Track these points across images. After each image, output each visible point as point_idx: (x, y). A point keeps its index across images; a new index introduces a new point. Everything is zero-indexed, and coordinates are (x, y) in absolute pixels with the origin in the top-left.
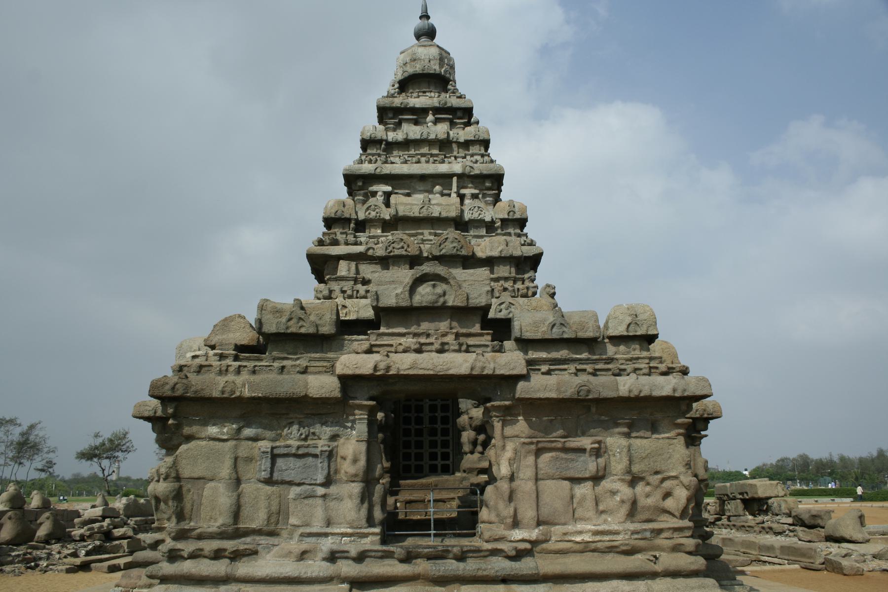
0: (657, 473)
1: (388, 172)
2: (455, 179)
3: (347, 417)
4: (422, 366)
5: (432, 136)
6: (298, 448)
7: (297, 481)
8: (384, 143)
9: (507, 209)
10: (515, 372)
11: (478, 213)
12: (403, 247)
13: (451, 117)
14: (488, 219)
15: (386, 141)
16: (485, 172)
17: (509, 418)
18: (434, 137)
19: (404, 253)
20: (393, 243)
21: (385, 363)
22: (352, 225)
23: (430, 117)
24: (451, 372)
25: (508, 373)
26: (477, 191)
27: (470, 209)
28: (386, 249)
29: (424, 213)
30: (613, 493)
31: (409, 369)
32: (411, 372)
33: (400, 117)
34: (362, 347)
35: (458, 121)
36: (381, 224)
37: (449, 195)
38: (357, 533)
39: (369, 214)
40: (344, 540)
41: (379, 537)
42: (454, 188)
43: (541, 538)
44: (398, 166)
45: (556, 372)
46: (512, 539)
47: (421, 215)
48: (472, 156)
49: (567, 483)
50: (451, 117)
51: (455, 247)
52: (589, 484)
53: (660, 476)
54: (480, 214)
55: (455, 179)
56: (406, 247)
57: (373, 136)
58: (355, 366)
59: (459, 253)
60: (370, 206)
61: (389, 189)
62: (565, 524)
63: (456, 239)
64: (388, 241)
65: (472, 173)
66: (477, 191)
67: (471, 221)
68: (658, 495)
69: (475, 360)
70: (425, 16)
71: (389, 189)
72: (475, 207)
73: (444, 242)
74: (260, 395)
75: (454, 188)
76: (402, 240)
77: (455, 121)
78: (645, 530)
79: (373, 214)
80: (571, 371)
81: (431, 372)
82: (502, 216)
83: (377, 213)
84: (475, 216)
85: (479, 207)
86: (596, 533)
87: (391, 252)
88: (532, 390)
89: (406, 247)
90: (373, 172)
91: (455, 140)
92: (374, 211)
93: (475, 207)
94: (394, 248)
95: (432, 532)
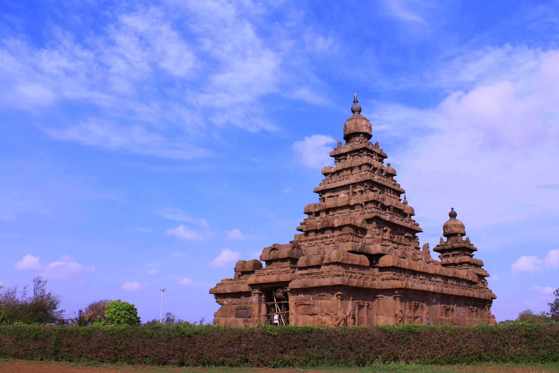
6: (243, 306)
7: (243, 317)
10: (287, 280)
16: (363, 180)
19: (312, 229)
22: (314, 215)
29: (336, 205)
32: (263, 282)
57: (325, 172)
59: (328, 226)
65: (358, 182)
67: (355, 205)
81: (266, 282)
84: (356, 202)
85: (357, 198)
87: (308, 229)
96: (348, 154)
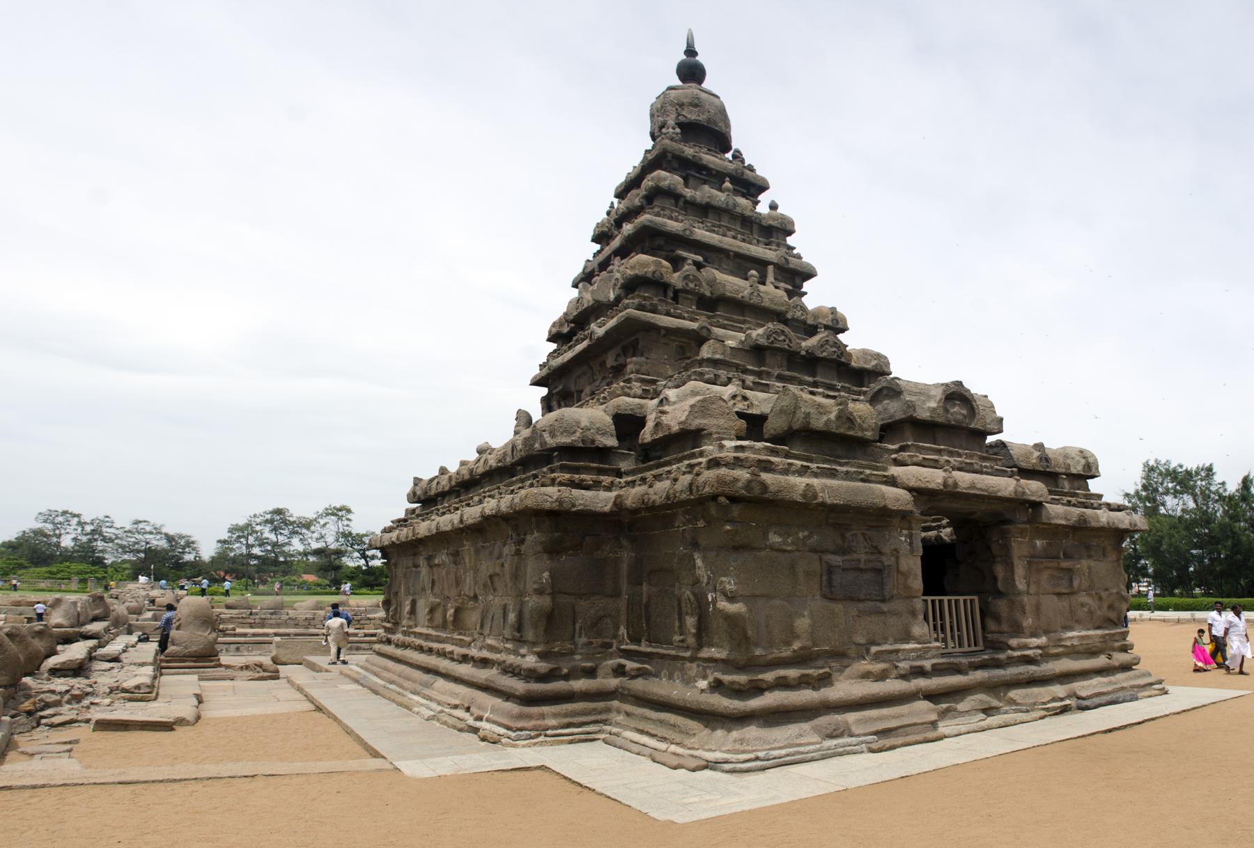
1: (698, 238)
2: (771, 268)
3: (901, 531)
4: (978, 486)
5: (738, 210)
8: (683, 199)
9: (831, 317)
11: (800, 313)
12: (785, 341)
13: (745, 191)
15: (685, 197)
18: (740, 212)
20: (774, 333)
22: (671, 294)
26: (790, 287)
28: (768, 339)
29: (755, 300)
31: (968, 488)
33: (689, 171)
34: (914, 459)
36: (696, 298)
50: (745, 191)
51: (835, 352)
54: (802, 314)
55: (771, 268)
58: (926, 480)
60: (688, 275)
61: (700, 258)
64: (769, 330)
66: (790, 287)
71: (700, 258)
72: (797, 305)
76: (783, 331)
79: (692, 285)
82: (825, 323)
83: (696, 286)
90: (681, 233)
91: (758, 221)
92: (691, 282)
96: (728, 179)
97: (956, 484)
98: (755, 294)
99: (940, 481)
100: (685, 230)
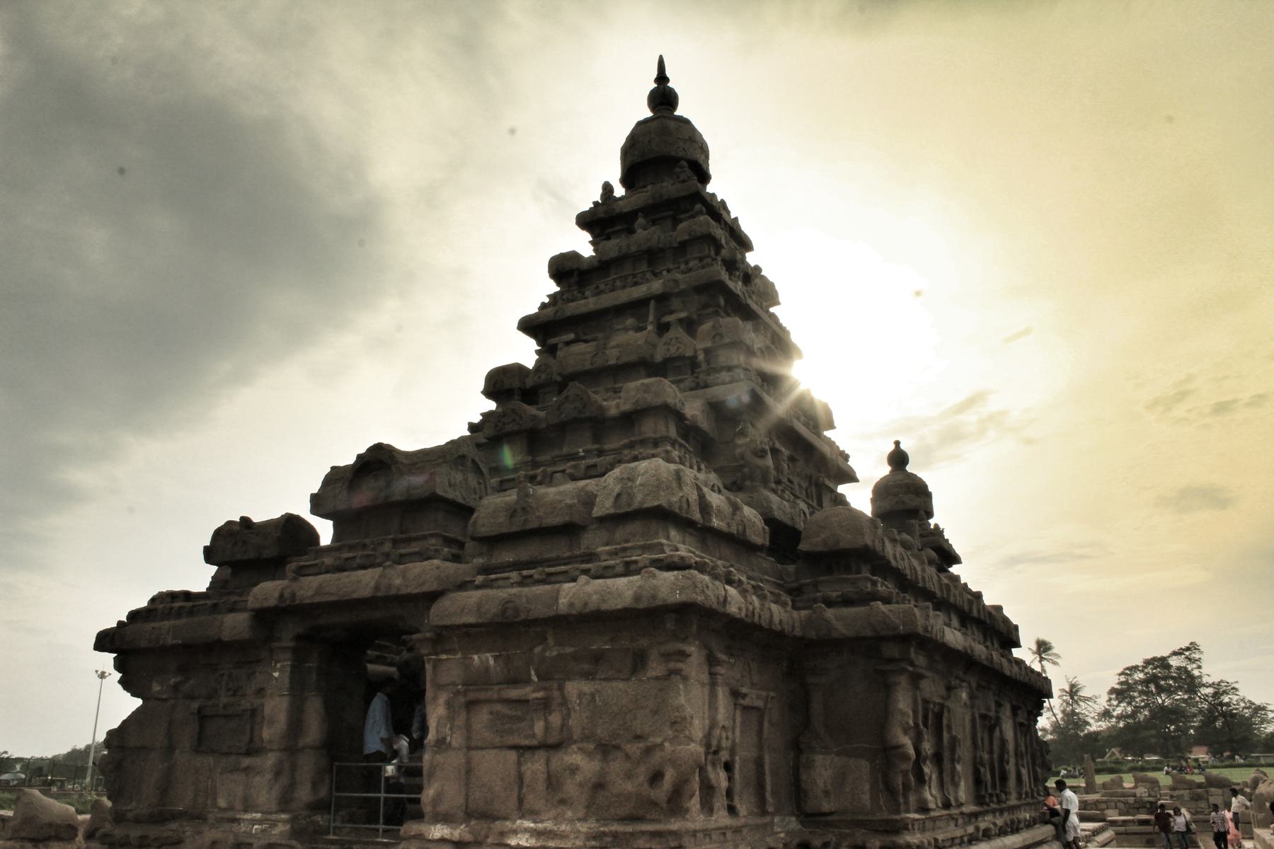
0: (638, 738)
3: (276, 665)
5: (633, 249)
8: (576, 273)
11: (676, 347)
12: (514, 420)
13: (671, 213)
14: (689, 353)
17: (444, 657)
19: (516, 428)
20: (504, 416)
21: (289, 590)
23: (641, 221)
24: (355, 596)
25: (416, 591)
27: (665, 344)
29: (599, 362)
30: (574, 770)
31: (313, 596)
32: (317, 600)
35: (682, 216)
37: (644, 329)
38: (266, 820)
39: (540, 377)
40: (256, 829)
41: (288, 827)
42: (651, 318)
43: (468, 837)
44: (589, 303)
45: (500, 583)
46: (430, 837)
47: (595, 366)
48: (687, 263)
49: (512, 755)
50: (671, 213)
52: (541, 756)
53: (642, 745)
54: (678, 348)
55: (652, 303)
56: (517, 419)
62: (505, 819)
63: (578, 395)
68: (642, 773)
69: (381, 576)
70: (662, 78)
72: (671, 339)
73: (563, 404)
74: (180, 642)
75: (651, 318)
77: (678, 217)
78: (604, 834)
80: (512, 581)
83: (548, 374)
84: (673, 351)
85: (677, 338)
86: (537, 834)
88: (447, 613)
89: (517, 419)
93: (671, 339)
94: (504, 424)
95: (381, 827)
97: (293, 595)
98: (600, 354)
99: (277, 595)
100: (556, 313)
